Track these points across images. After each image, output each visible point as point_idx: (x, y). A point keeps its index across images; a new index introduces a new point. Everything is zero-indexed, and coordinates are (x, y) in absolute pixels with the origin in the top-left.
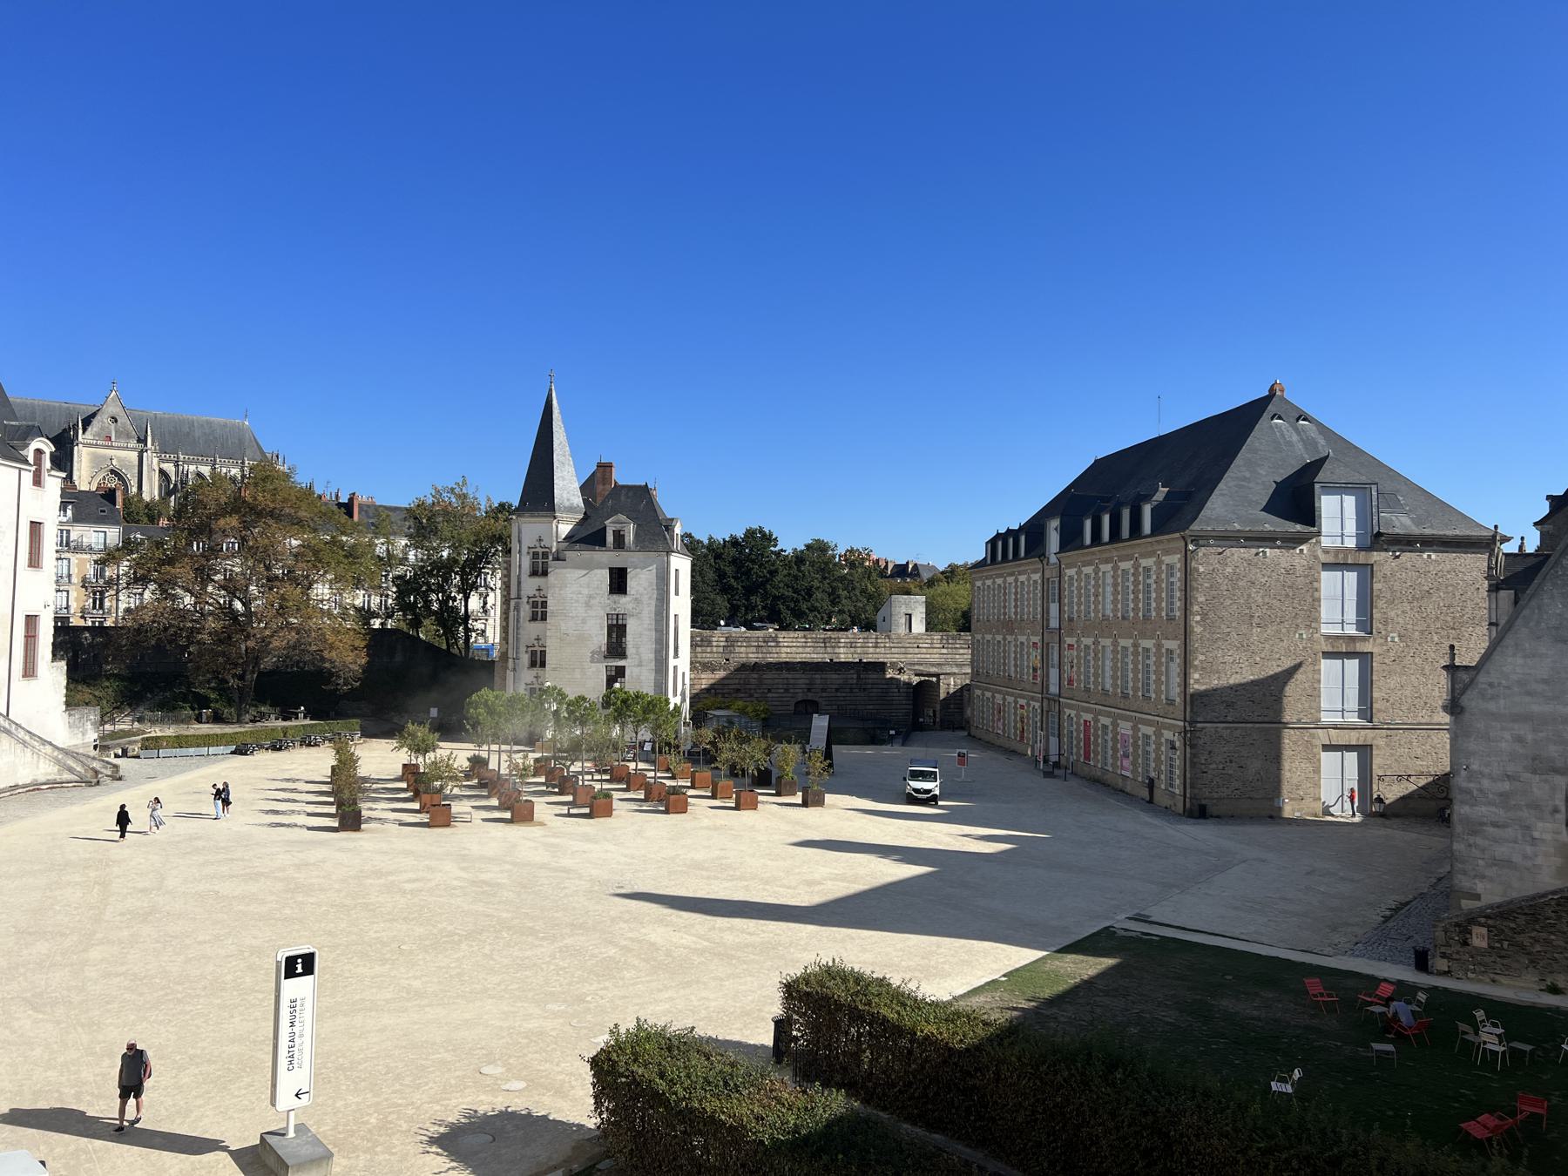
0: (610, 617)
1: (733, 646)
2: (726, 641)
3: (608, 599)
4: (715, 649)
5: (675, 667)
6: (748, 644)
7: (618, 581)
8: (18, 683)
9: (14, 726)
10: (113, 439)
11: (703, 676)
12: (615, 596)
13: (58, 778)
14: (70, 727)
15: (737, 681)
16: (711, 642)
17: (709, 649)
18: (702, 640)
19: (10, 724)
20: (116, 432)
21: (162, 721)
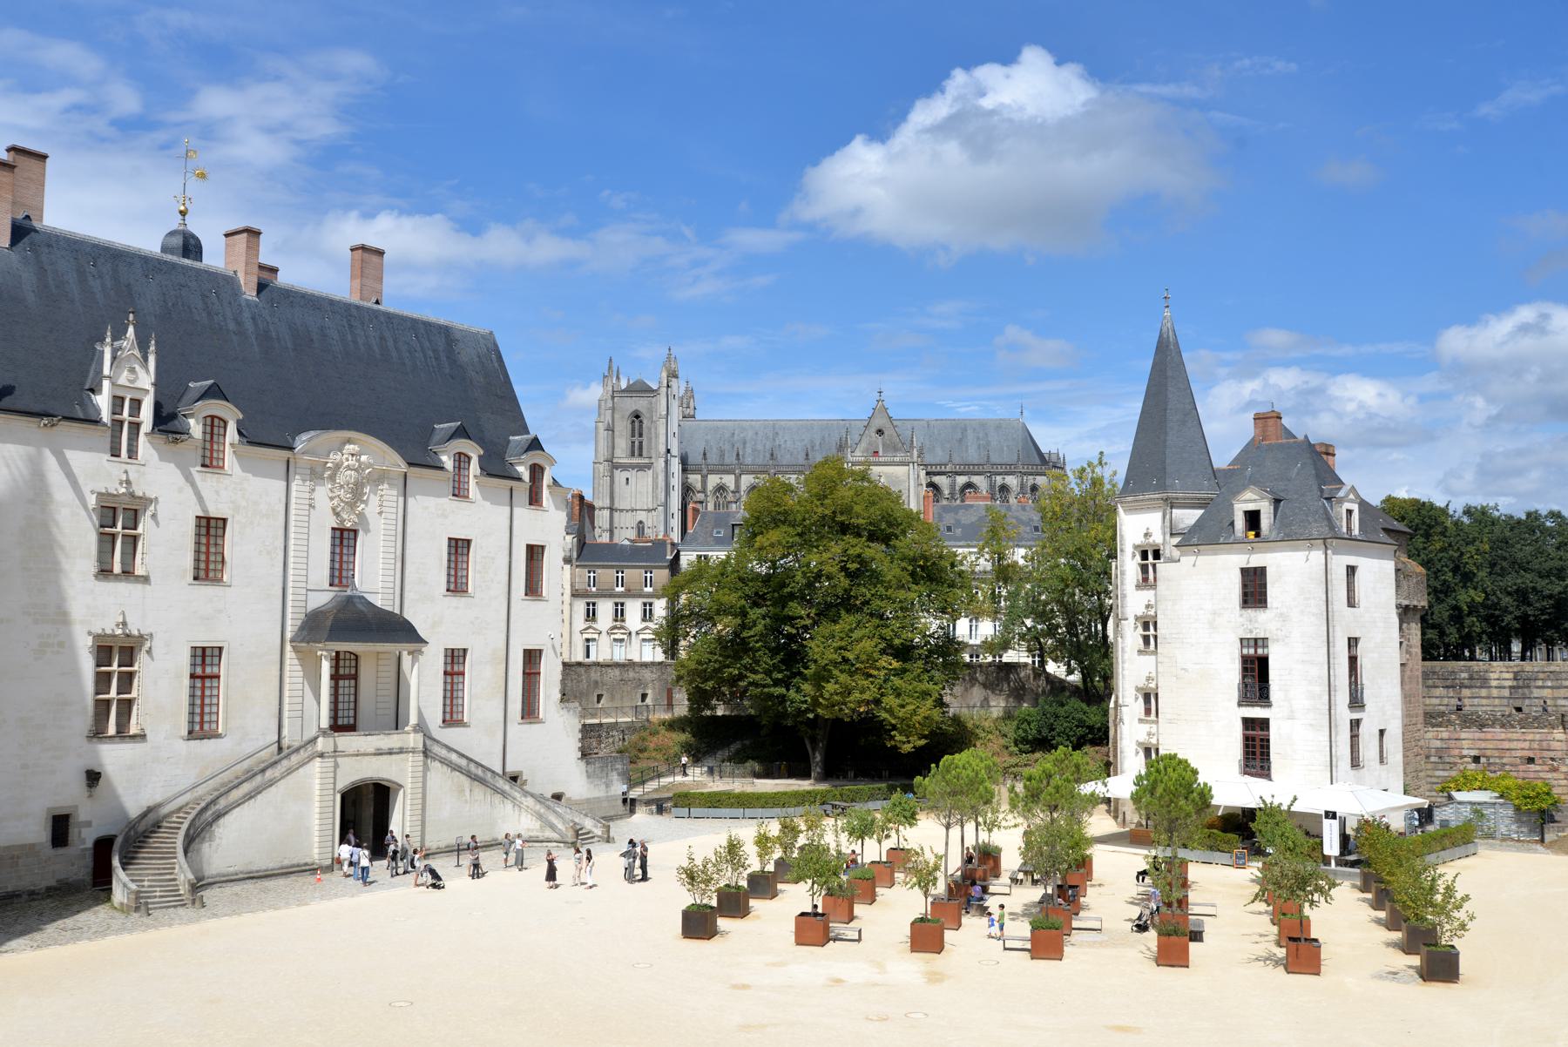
0: (1245, 643)
1: (1529, 687)
2: (1515, 679)
3: (1241, 615)
4: (1495, 692)
5: (1355, 724)
6: (1555, 683)
7: (1254, 589)
8: (517, 729)
9: (489, 774)
10: (881, 453)
11: (1463, 735)
12: (1249, 611)
13: (541, 835)
14: (588, 777)
15: (1527, 745)
16: (1486, 680)
17: (1484, 692)
18: (1471, 678)
19: (484, 772)
20: (883, 445)
21: (732, 775)
